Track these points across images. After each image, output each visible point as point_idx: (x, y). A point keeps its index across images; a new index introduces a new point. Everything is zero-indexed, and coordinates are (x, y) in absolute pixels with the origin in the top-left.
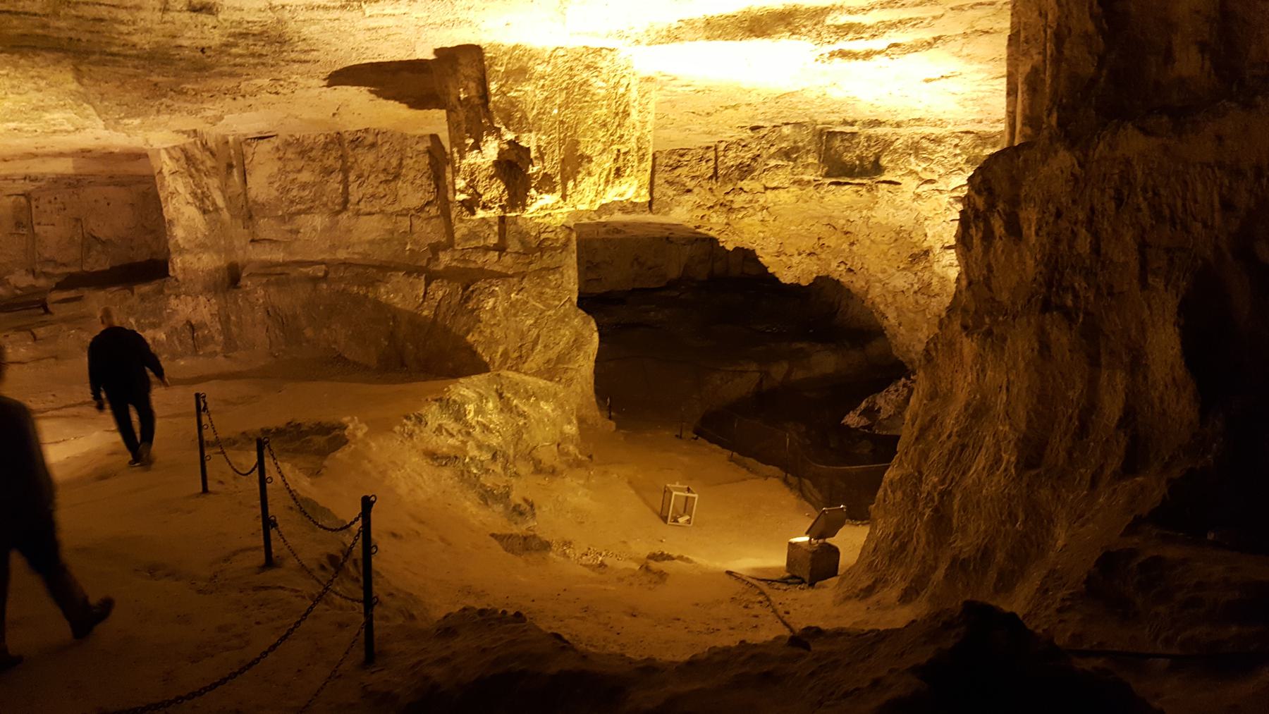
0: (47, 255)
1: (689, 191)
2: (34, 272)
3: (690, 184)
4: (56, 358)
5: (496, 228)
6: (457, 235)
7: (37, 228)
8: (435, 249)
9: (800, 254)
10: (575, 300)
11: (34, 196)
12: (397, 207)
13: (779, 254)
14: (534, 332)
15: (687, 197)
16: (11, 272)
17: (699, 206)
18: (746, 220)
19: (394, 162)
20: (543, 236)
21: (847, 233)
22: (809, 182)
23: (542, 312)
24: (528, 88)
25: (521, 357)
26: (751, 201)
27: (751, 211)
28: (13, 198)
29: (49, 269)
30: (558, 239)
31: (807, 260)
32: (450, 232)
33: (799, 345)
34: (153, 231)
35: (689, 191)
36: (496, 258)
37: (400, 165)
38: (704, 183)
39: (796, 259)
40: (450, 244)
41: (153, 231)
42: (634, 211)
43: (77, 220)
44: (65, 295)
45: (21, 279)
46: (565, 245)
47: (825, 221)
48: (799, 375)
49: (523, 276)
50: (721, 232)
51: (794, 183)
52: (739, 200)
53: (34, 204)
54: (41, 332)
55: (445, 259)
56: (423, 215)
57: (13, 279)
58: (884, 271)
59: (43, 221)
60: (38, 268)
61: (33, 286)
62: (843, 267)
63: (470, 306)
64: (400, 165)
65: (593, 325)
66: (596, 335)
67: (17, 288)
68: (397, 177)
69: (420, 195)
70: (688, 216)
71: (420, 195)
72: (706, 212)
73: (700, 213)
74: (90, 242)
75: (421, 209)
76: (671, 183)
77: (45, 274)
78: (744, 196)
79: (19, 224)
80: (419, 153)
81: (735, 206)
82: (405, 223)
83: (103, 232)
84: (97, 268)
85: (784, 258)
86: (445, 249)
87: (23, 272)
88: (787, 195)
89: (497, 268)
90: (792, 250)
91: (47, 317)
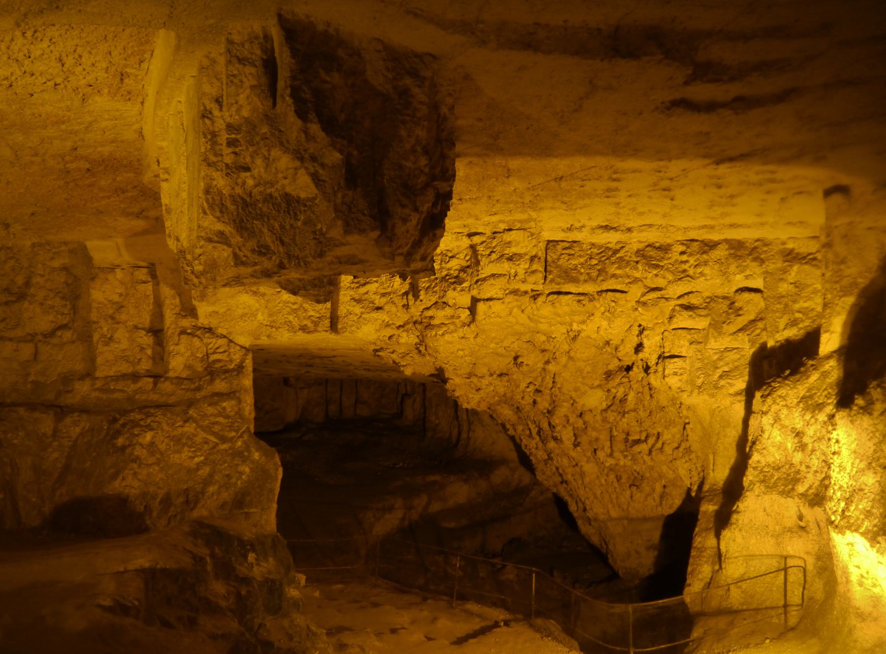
1: (379, 308)
3: (379, 301)
5: (149, 352)
6: (99, 360)
8: (67, 380)
9: (491, 375)
10: (252, 430)
12: (19, 332)
13: (470, 375)
14: (205, 471)
15: (375, 315)
17: (388, 325)
18: (447, 337)
19: (20, 280)
20: (213, 358)
21: (543, 351)
22: (526, 292)
23: (217, 444)
24: (336, 78)
25: (187, 502)
26: (453, 317)
27: (452, 327)
30: (231, 361)
31: (497, 382)
32: (93, 360)
33: (431, 478)
35: (379, 308)
36: (151, 385)
37: (27, 284)
38: (396, 300)
39: (485, 382)
40: (89, 374)
42: (316, 331)
46: (240, 368)
47: (527, 337)
48: (436, 507)
49: (191, 403)
50: (404, 356)
51: (511, 293)
52: (440, 316)
55: (83, 389)
56: (55, 341)
58: (576, 390)
62: (532, 388)
63: (120, 441)
64: (27, 284)
65: (277, 459)
66: (281, 470)
68: (21, 297)
69: (51, 318)
70: (376, 337)
71: (51, 318)
72: (396, 332)
73: (389, 332)
75: (52, 334)
76: (359, 301)
78: (448, 311)
80: (54, 269)
81: (435, 322)
82: (27, 350)
85: (474, 379)
86: (82, 378)
88: (503, 307)
89: (154, 397)
90: (484, 371)
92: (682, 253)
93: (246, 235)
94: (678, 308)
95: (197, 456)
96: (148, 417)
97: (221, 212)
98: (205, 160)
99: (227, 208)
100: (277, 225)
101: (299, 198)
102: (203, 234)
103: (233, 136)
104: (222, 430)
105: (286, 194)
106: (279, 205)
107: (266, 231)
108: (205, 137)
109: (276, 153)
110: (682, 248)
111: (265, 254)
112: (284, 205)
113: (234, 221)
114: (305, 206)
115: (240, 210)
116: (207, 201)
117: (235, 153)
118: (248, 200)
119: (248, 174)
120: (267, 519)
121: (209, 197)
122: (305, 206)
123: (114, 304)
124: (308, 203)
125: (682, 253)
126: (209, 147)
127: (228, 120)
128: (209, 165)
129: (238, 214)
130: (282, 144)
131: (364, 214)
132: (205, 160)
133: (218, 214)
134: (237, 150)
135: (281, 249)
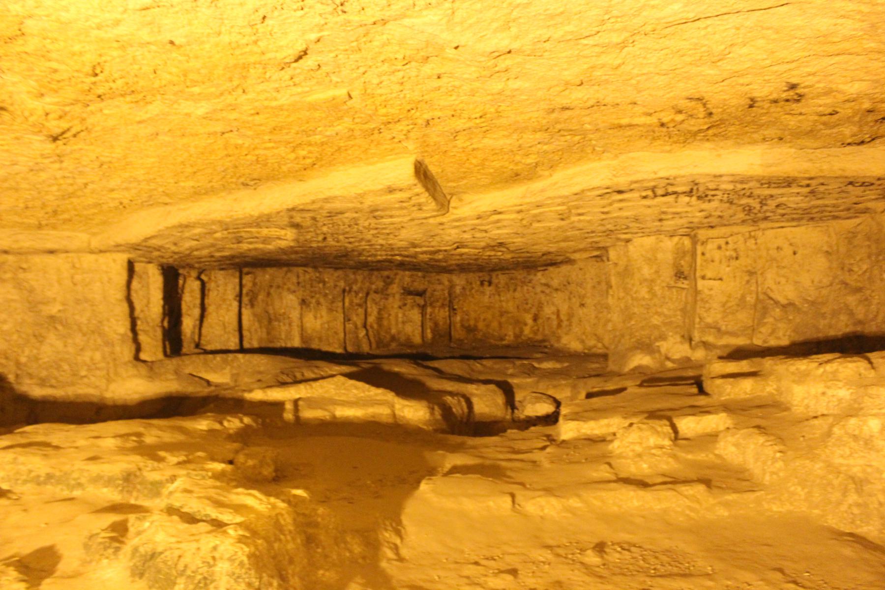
0: (709, 320)
2: (691, 340)
4: (707, 482)
7: (701, 284)
11: (702, 234)
16: (663, 337)
28: (676, 239)
29: (710, 339)
34: (859, 290)
41: (859, 290)
43: (751, 273)
44: (732, 367)
45: (675, 349)
53: (700, 249)
54: (688, 425)
57: (663, 346)
59: (709, 274)
60: (697, 336)
61: (688, 359)
67: (668, 359)
74: (763, 305)
77: (706, 345)
79: (680, 275)
83: (786, 292)
84: (773, 342)
87: (678, 338)
91: (702, 401)
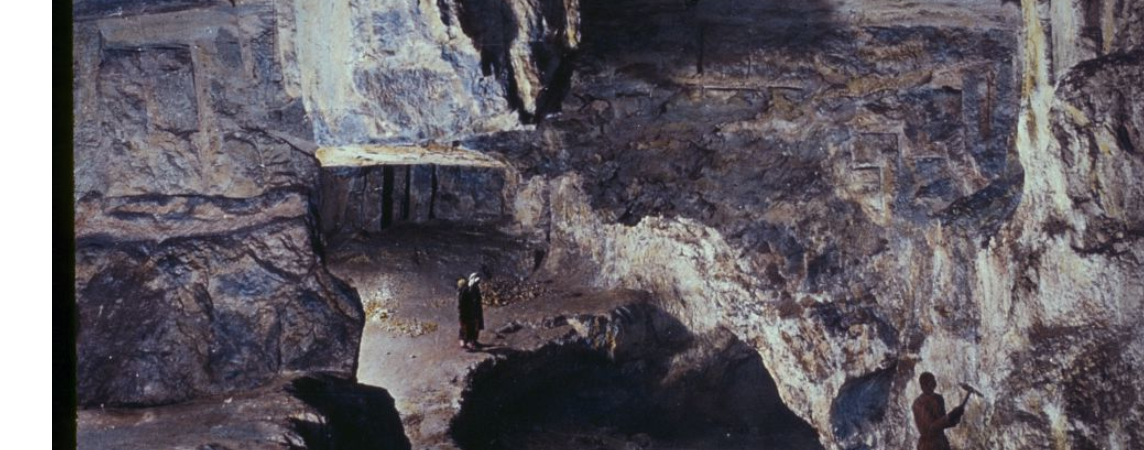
92: (869, 43)
93: (389, 109)
94: (865, 109)
95: (256, 301)
96: (191, 251)
97: (367, 90)
98: (353, 46)
99: (372, 86)
100: (416, 98)
101: (436, 72)
102: (348, 108)
103: (379, 24)
104: (288, 266)
105: (425, 70)
106: (418, 80)
107: (406, 103)
108: (353, 24)
109: (421, 43)
110: (869, 37)
111: (406, 125)
112: (422, 79)
113: (379, 98)
114: (442, 80)
115: (384, 88)
116: (355, 80)
117: (382, 40)
118: (390, 76)
119: (392, 58)
120: (533, 334)
121: (357, 77)
122: (442, 80)
123: (127, 97)
124: (445, 78)
125: (869, 43)
126: (356, 33)
127: (374, 9)
128: (358, 50)
129: (383, 91)
130: (425, 36)
131: (498, 95)
132: (353, 46)
133: (364, 91)
134: (383, 37)
135: (421, 120)
